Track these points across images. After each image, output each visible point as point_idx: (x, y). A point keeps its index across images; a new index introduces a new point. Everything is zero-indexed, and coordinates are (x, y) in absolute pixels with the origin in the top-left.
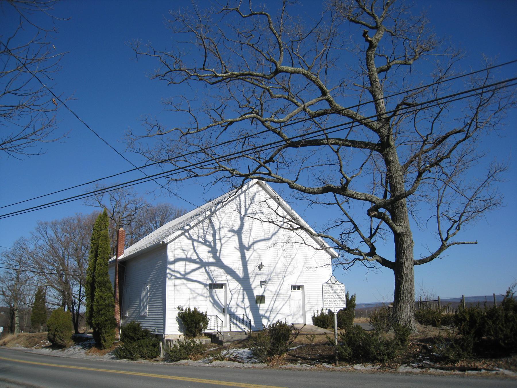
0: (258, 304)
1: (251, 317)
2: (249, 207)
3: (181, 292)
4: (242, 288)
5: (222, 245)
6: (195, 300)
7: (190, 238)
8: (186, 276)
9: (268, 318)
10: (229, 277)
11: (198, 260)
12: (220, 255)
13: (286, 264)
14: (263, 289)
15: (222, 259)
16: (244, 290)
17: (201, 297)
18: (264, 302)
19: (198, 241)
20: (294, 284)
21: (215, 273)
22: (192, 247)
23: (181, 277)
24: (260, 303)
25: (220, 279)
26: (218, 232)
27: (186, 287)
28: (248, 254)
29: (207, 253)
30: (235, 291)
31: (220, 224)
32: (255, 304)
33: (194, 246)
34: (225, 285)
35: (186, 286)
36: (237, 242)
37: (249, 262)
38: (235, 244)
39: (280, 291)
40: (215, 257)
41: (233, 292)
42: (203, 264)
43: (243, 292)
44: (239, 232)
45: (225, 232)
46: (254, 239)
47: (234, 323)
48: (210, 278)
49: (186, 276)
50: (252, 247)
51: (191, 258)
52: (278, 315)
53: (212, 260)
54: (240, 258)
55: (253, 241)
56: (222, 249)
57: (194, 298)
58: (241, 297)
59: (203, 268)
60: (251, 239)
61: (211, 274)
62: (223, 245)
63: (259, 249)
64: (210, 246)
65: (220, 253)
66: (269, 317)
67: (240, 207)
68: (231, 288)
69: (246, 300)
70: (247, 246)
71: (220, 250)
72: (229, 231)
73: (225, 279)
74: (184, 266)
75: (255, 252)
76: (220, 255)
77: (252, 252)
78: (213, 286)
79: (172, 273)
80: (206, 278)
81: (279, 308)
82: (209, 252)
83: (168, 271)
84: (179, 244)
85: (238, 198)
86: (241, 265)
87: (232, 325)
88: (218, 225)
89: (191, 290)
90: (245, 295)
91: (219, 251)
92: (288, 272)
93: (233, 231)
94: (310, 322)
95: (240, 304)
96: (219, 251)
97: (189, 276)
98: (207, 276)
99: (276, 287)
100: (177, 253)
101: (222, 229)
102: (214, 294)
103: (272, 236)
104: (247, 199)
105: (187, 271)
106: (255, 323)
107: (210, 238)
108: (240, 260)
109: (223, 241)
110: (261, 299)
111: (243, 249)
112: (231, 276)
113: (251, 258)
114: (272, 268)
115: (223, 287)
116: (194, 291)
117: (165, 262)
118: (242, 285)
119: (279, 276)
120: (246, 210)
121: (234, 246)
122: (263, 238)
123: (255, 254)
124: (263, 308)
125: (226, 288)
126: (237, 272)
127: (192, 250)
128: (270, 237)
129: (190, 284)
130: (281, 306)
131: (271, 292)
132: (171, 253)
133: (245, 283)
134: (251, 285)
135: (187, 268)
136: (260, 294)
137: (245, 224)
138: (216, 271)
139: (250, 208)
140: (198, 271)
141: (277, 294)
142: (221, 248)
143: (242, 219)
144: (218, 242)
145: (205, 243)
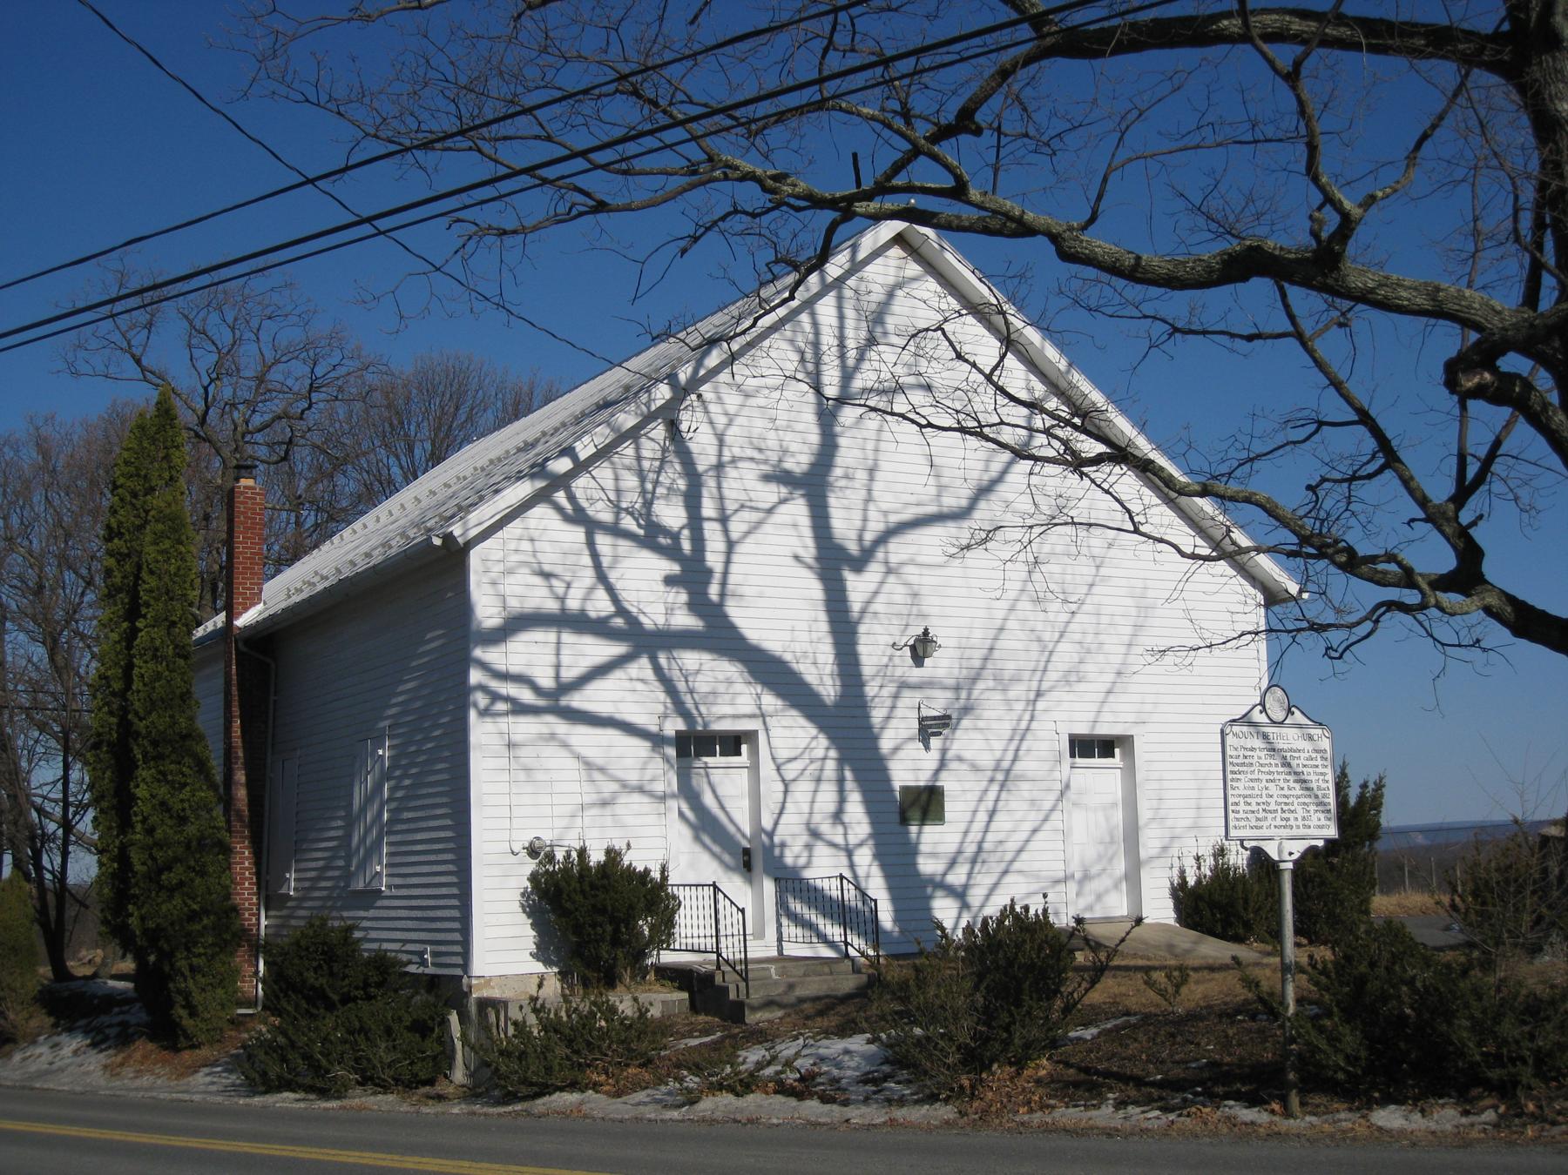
0: (914, 829)
1: (877, 888)
2: (861, 359)
3: (539, 776)
4: (833, 753)
5: (731, 545)
6: (608, 810)
7: (578, 516)
8: (564, 701)
9: (960, 895)
10: (770, 701)
11: (619, 622)
12: (722, 595)
13: (1047, 636)
14: (934, 755)
15: (736, 613)
16: (841, 761)
17: (636, 797)
18: (939, 818)
19: (616, 531)
20: (1082, 729)
21: (702, 685)
23: (541, 702)
24: (923, 823)
25: (728, 710)
26: (711, 483)
27: (563, 753)
28: (858, 586)
29: (662, 587)
30: (798, 765)
31: (721, 443)
32: (899, 828)
33: (595, 556)
34: (750, 737)
35: (565, 745)
36: (807, 532)
37: (862, 629)
38: (795, 541)
39: (1019, 766)
40: (699, 604)
41: (790, 771)
43: (840, 770)
44: (813, 485)
45: (744, 484)
46: (886, 513)
47: (797, 920)
49: (564, 701)
50: (880, 555)
51: (583, 612)
52: (1009, 879)
53: (684, 620)
54: (821, 606)
55: (881, 527)
56: (733, 568)
57: (604, 804)
58: (827, 797)
59: (644, 661)
60: (873, 514)
61: (681, 686)
62: (739, 548)
63: (912, 562)
64: (672, 552)
65: (724, 584)
66: (966, 887)
67: (818, 363)
68: (783, 754)
69: (855, 808)
70: (853, 548)
71: (726, 573)
72: (767, 478)
73: (750, 709)
74: (551, 649)
75: (892, 579)
77: (877, 577)
78: (696, 744)
79: (495, 685)
80: (661, 709)
81: (1012, 846)
82: (670, 581)
83: (475, 676)
84: (526, 546)
85: (804, 318)
86: (829, 640)
87: (790, 930)
88: (713, 450)
89: (589, 766)
91: (717, 577)
92: (1052, 676)
94: (1160, 910)
95: (825, 828)
96: (717, 577)
97: (577, 701)
98: (662, 696)
99: (999, 745)
100: (519, 590)
101: (731, 472)
102: (699, 782)
104: (850, 323)
105: (569, 674)
106: (896, 920)
107: (672, 515)
108: (823, 616)
109: (737, 527)
110: (926, 803)
111: (833, 562)
112: (779, 695)
113: (874, 607)
115: (744, 748)
116: (601, 769)
117: (460, 634)
118: (835, 740)
119: (1012, 694)
120: (847, 376)
121: (788, 551)
122: (931, 509)
123: (894, 588)
124: (935, 844)
125: (754, 753)
126: (811, 677)
127: (588, 576)
128: (964, 503)
129: (585, 738)
130: (1024, 836)
131: (975, 768)
132: (488, 589)
133: (847, 725)
134: (875, 739)
135: (565, 660)
136: (922, 780)
137: (842, 441)
138: (706, 672)
139: (866, 365)
140: (618, 674)
141: (1004, 777)
142: (728, 562)
143: (827, 416)
144: (712, 531)
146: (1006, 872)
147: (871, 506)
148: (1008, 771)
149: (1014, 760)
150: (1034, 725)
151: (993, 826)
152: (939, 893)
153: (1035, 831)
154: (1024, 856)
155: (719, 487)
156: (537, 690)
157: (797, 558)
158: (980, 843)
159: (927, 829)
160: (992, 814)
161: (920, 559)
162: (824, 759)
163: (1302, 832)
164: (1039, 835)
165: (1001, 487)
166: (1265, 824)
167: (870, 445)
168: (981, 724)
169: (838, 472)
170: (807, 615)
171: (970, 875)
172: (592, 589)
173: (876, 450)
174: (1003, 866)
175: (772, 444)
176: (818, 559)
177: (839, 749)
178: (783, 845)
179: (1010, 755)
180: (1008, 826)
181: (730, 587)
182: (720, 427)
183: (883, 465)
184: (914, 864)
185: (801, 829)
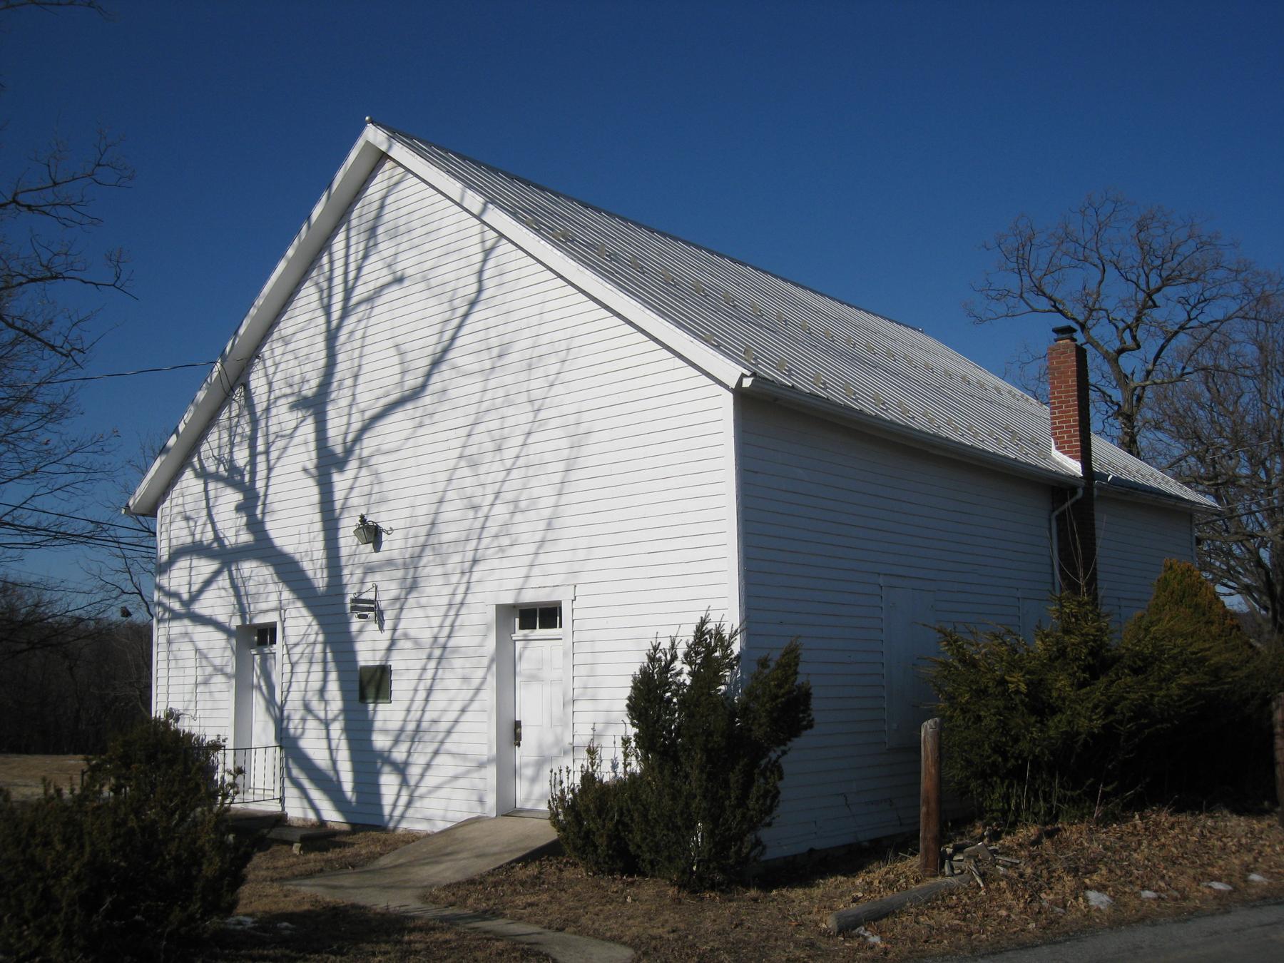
0: (371, 706)
1: (343, 756)
2: (357, 278)
4: (321, 638)
9: (401, 769)
12: (263, 513)
14: (387, 634)
16: (325, 643)
19: (216, 477)
20: (509, 599)
22: (204, 504)
24: (375, 703)
26: (263, 423)
36: (312, 446)
38: (305, 457)
39: (452, 643)
42: (226, 556)
43: (324, 652)
45: (283, 417)
48: (243, 612)
52: (439, 760)
53: (245, 538)
56: (271, 490)
58: (316, 676)
65: (264, 504)
66: (406, 764)
67: (330, 296)
68: (292, 640)
69: (333, 687)
71: (266, 495)
72: (294, 407)
75: (364, 472)
79: (165, 600)
81: (444, 726)
85: (325, 259)
87: (291, 792)
88: (265, 397)
90: (331, 666)
92: (485, 542)
93: (302, 403)
95: (316, 705)
98: (233, 600)
99: (436, 622)
101: (274, 411)
103: (429, 375)
105: (195, 588)
106: (355, 789)
107: (241, 457)
109: (274, 455)
114: (424, 531)
119: (449, 568)
128: (420, 381)
130: (452, 716)
138: (254, 572)
139: (360, 282)
141: (440, 652)
145: (233, 477)
146: (436, 753)
147: (354, 410)
148: (444, 647)
149: (449, 637)
150: (470, 598)
151: (430, 706)
152: (387, 769)
153: (463, 711)
154: (454, 737)
155: (267, 427)
156: (183, 603)
157: (305, 470)
158: (419, 722)
159: (381, 707)
160: (430, 691)
161: (385, 448)
162: (314, 643)
164: (467, 716)
165: (451, 355)
167: (356, 353)
168: (424, 601)
169: (335, 385)
170: (306, 519)
171: (409, 753)
172: (205, 524)
173: (361, 357)
174: (435, 745)
175: (297, 379)
176: (317, 467)
177: (325, 633)
178: (289, 718)
179: (446, 631)
180: (441, 705)
183: (365, 369)
184: (370, 741)
185: (299, 704)
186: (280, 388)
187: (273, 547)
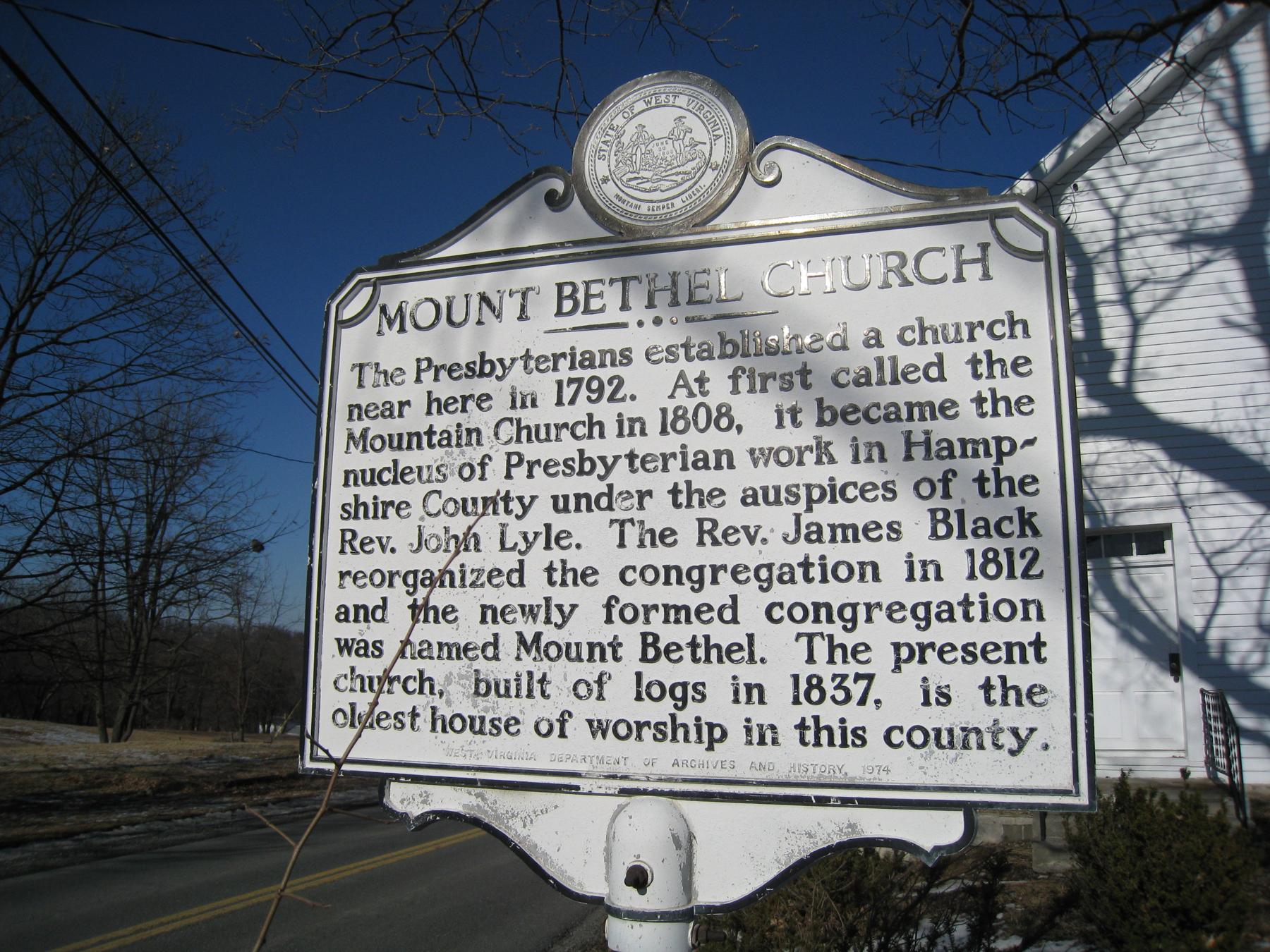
5: (1136, 323)
12: (1130, 370)
15: (1150, 395)
31: (1116, 218)
45: (1153, 256)
56: (1142, 341)
71: (1133, 347)
76: (1130, 370)
96: (1122, 354)
109: (1142, 303)
163: (790, 759)
166: (531, 710)
181: (1139, 363)
182: (1114, 202)
186: (1135, 215)
187: (1151, 415)
